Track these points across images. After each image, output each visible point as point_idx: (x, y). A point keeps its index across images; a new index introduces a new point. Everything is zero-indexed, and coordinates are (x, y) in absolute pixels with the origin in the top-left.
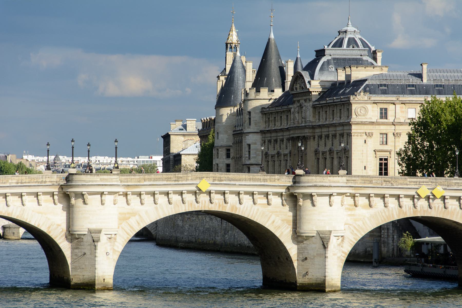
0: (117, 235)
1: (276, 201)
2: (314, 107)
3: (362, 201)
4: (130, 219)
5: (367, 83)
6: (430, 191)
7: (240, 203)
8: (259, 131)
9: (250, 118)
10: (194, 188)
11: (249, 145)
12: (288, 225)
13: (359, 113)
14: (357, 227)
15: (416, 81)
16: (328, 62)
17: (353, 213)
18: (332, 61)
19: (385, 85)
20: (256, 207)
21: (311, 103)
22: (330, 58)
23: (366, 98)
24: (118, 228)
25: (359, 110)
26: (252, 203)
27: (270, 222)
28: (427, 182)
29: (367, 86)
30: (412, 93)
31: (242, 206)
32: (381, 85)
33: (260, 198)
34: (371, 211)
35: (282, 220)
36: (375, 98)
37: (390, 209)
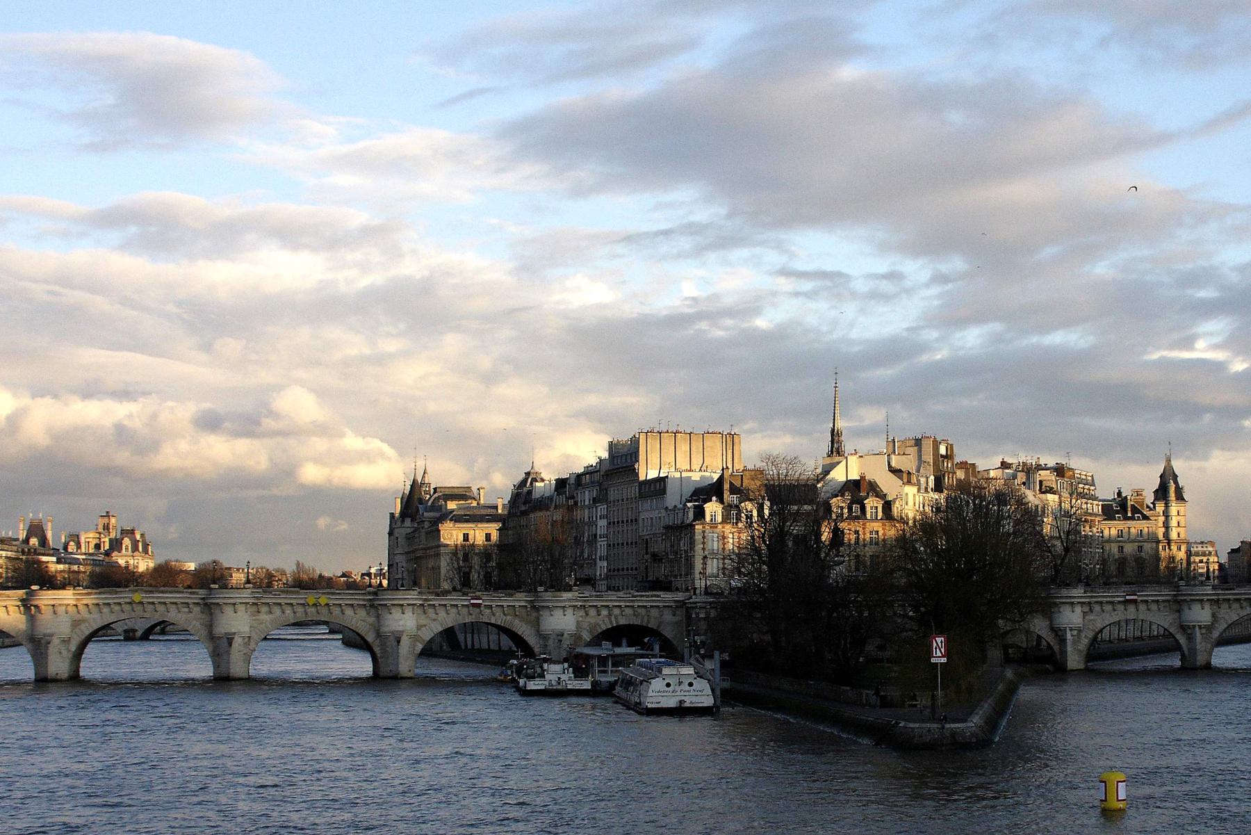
1: (197, 609)
2: (427, 533)
3: (264, 609)
5: (454, 513)
9: (397, 543)
11: (397, 563)
15: (492, 511)
17: (257, 617)
20: (180, 615)
22: (440, 494)
23: (451, 525)
26: (177, 611)
27: (191, 627)
30: (489, 521)
31: (169, 614)
32: (465, 515)
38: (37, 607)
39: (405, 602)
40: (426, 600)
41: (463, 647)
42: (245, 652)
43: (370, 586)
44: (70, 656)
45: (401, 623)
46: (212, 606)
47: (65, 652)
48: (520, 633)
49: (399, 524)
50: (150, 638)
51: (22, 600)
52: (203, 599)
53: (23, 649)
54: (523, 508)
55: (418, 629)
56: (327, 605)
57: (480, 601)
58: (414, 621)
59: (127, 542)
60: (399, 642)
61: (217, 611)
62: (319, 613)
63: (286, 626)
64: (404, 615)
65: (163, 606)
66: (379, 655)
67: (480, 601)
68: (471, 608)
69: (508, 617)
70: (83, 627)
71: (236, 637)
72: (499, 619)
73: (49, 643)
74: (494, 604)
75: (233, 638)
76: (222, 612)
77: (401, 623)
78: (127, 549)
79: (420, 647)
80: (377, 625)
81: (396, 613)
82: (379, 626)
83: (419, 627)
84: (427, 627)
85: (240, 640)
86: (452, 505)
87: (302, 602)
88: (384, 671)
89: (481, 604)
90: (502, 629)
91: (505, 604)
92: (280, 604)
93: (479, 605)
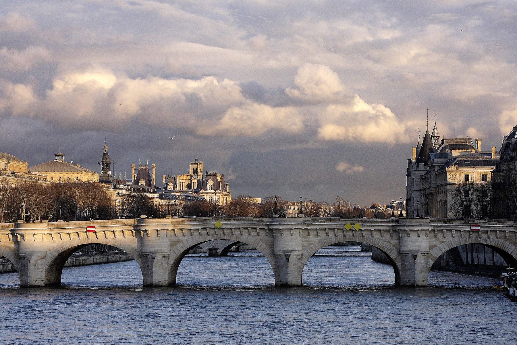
0: (170, 255)
1: (263, 233)
3: (313, 233)
4: (177, 245)
6: (352, 226)
7: (241, 235)
8: (419, 190)
10: (213, 226)
11: (414, 198)
12: (269, 248)
13: (452, 178)
14: (310, 248)
15: (488, 158)
16: (446, 147)
18: (448, 147)
19: (468, 161)
21: (434, 172)
22: (447, 144)
24: (171, 250)
25: (451, 176)
28: (352, 221)
29: (458, 161)
30: (485, 165)
31: (242, 237)
32: (466, 161)
33: (252, 231)
34: (319, 238)
35: (266, 245)
36: (460, 168)
37: (330, 237)
38: (145, 231)
39: (420, 228)
40: (435, 226)
41: (465, 262)
42: (299, 265)
43: (393, 215)
44: (169, 268)
45: (417, 244)
46: (274, 231)
47: (165, 265)
48: (509, 252)
49: (415, 167)
50: (228, 254)
51: (135, 226)
52: (267, 225)
53: (134, 263)
54: (512, 155)
55: (430, 249)
56: (360, 230)
57: (478, 228)
58: (427, 243)
59: (210, 182)
60: (415, 259)
61: (278, 235)
62: (354, 236)
63: (329, 246)
64: (419, 238)
65: (238, 230)
66: (399, 269)
67: (478, 228)
68: (471, 233)
69: (501, 240)
70: (178, 246)
71: (292, 254)
72: (493, 241)
73: (154, 258)
74: (489, 230)
75: (290, 255)
76: (282, 236)
77: (417, 244)
78: (211, 188)
79: (431, 262)
80: (398, 246)
81: (413, 236)
82: (400, 247)
83: (431, 247)
84: (437, 247)
85: (295, 256)
86: (456, 153)
87: (342, 228)
88: (405, 280)
89: (479, 230)
90: (495, 249)
91: (498, 230)
92: (325, 230)
93: (477, 231)
